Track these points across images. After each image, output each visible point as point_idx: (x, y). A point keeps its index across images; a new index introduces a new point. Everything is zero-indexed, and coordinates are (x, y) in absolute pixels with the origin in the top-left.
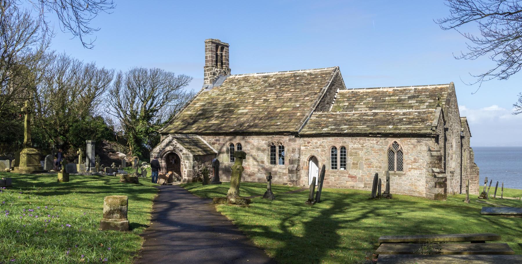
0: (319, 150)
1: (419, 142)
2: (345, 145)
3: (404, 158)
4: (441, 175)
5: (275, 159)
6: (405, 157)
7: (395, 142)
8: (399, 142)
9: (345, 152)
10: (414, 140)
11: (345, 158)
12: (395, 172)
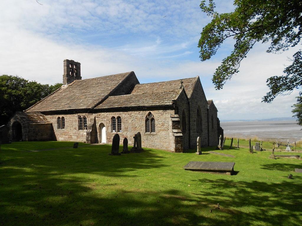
0: (105, 119)
2: (120, 116)
6: (156, 122)
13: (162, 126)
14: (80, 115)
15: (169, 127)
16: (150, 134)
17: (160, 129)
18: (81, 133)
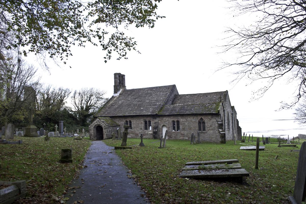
0: (167, 122)
1: (212, 117)
2: (179, 120)
3: (205, 125)
4: (223, 133)
5: (147, 127)
6: (206, 124)
7: (202, 118)
8: (203, 118)
9: (179, 123)
10: (210, 117)
11: (179, 126)
13: (210, 127)
14: (146, 119)
15: (216, 127)
17: (209, 129)
18: (146, 132)
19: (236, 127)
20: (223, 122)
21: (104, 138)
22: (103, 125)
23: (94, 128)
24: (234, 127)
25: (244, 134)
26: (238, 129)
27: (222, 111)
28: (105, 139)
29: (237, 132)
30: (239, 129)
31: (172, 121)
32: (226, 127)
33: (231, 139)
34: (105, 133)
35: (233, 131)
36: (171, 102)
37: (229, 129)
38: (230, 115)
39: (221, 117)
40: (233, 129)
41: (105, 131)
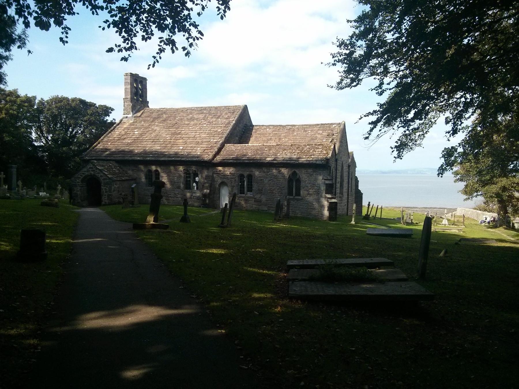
7: (295, 172)
8: (297, 171)
10: (310, 171)
11: (252, 185)
12: (294, 197)
16: (294, 199)
19: (354, 191)
20: (334, 180)
21: (103, 203)
22: (101, 176)
23: (82, 181)
24: (350, 190)
25: (369, 205)
26: (355, 195)
27: (334, 159)
28: (105, 205)
29: (354, 200)
30: (359, 196)
31: (238, 175)
32: (338, 191)
33: (344, 213)
34: (106, 192)
35: (348, 198)
36: (237, 138)
37: (342, 194)
38: (345, 168)
39: (331, 172)
40: (348, 195)
41: (105, 190)
